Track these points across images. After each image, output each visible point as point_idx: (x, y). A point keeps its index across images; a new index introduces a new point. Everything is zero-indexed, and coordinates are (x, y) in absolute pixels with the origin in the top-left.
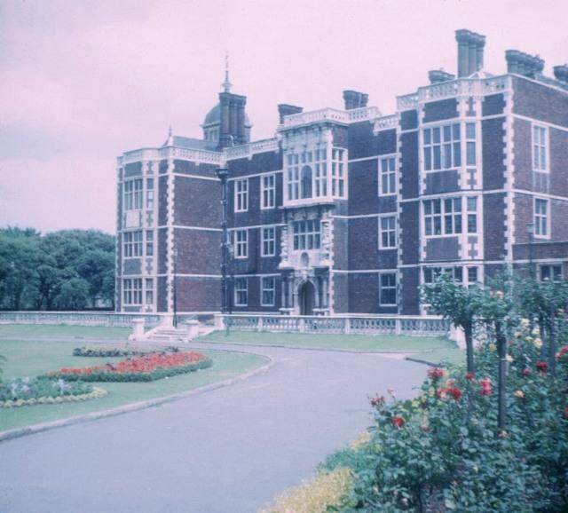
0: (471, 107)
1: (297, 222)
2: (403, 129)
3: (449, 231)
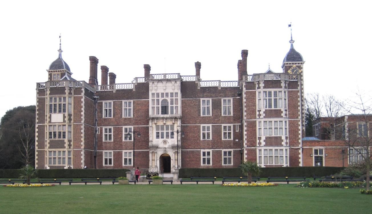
1: (159, 126)
2: (246, 89)
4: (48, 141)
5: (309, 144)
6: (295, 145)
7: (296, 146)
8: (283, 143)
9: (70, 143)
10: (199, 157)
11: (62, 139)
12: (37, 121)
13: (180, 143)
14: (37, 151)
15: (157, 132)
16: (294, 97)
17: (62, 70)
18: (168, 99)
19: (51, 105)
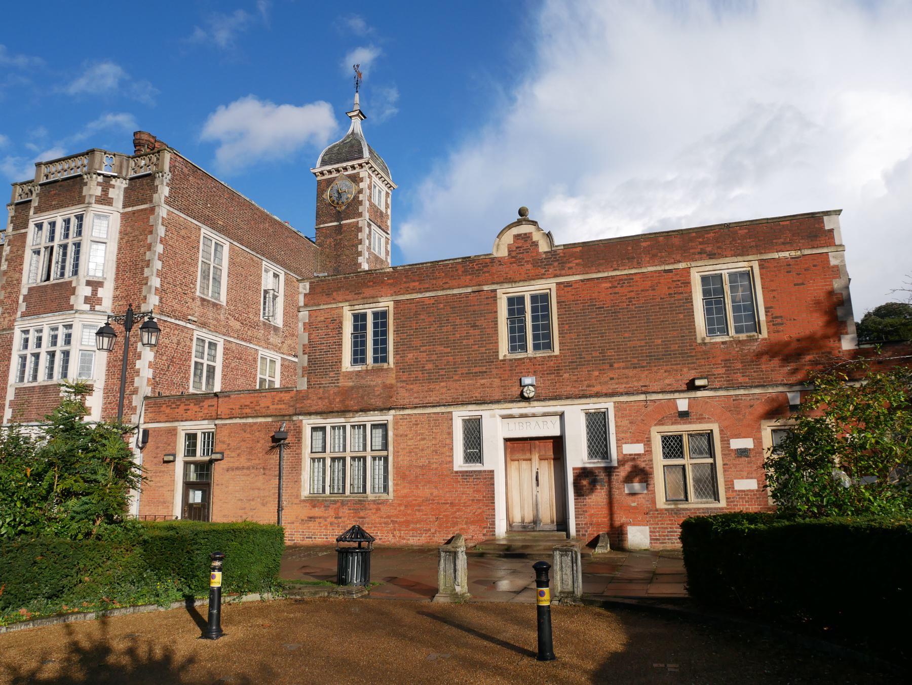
0: (105, 192)
2: (14, 229)
5: (168, 411)
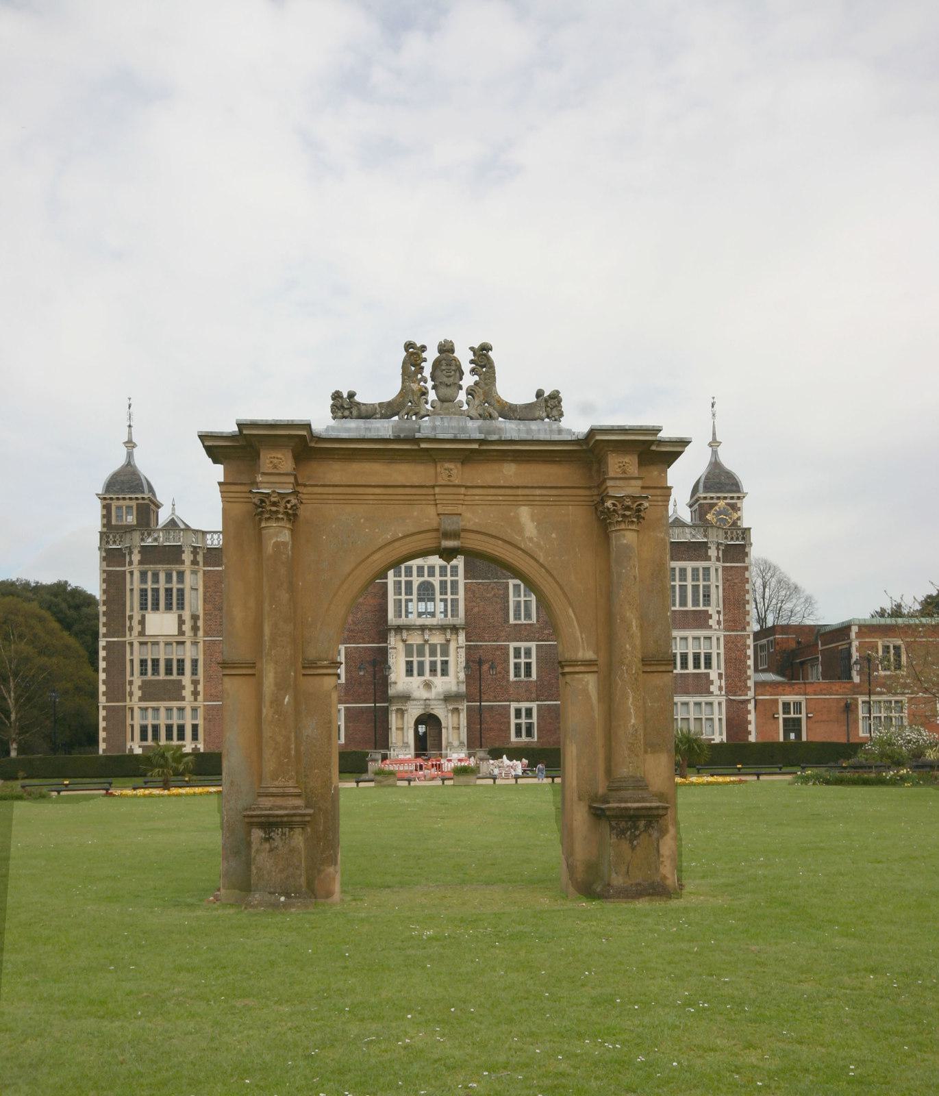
1: (411, 645)
3: (697, 666)
4: (137, 681)
5: (770, 690)
6: (740, 693)
7: (740, 695)
8: (712, 688)
9: (196, 688)
10: (505, 720)
11: (174, 677)
12: (102, 630)
13: (463, 688)
14: (104, 708)
15: (407, 661)
16: (736, 581)
17: (139, 496)
18: (434, 582)
19: (143, 592)
